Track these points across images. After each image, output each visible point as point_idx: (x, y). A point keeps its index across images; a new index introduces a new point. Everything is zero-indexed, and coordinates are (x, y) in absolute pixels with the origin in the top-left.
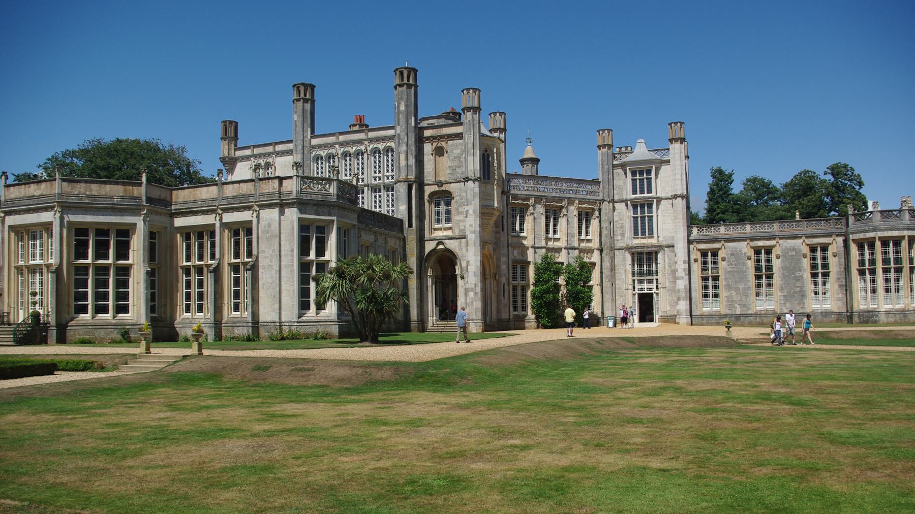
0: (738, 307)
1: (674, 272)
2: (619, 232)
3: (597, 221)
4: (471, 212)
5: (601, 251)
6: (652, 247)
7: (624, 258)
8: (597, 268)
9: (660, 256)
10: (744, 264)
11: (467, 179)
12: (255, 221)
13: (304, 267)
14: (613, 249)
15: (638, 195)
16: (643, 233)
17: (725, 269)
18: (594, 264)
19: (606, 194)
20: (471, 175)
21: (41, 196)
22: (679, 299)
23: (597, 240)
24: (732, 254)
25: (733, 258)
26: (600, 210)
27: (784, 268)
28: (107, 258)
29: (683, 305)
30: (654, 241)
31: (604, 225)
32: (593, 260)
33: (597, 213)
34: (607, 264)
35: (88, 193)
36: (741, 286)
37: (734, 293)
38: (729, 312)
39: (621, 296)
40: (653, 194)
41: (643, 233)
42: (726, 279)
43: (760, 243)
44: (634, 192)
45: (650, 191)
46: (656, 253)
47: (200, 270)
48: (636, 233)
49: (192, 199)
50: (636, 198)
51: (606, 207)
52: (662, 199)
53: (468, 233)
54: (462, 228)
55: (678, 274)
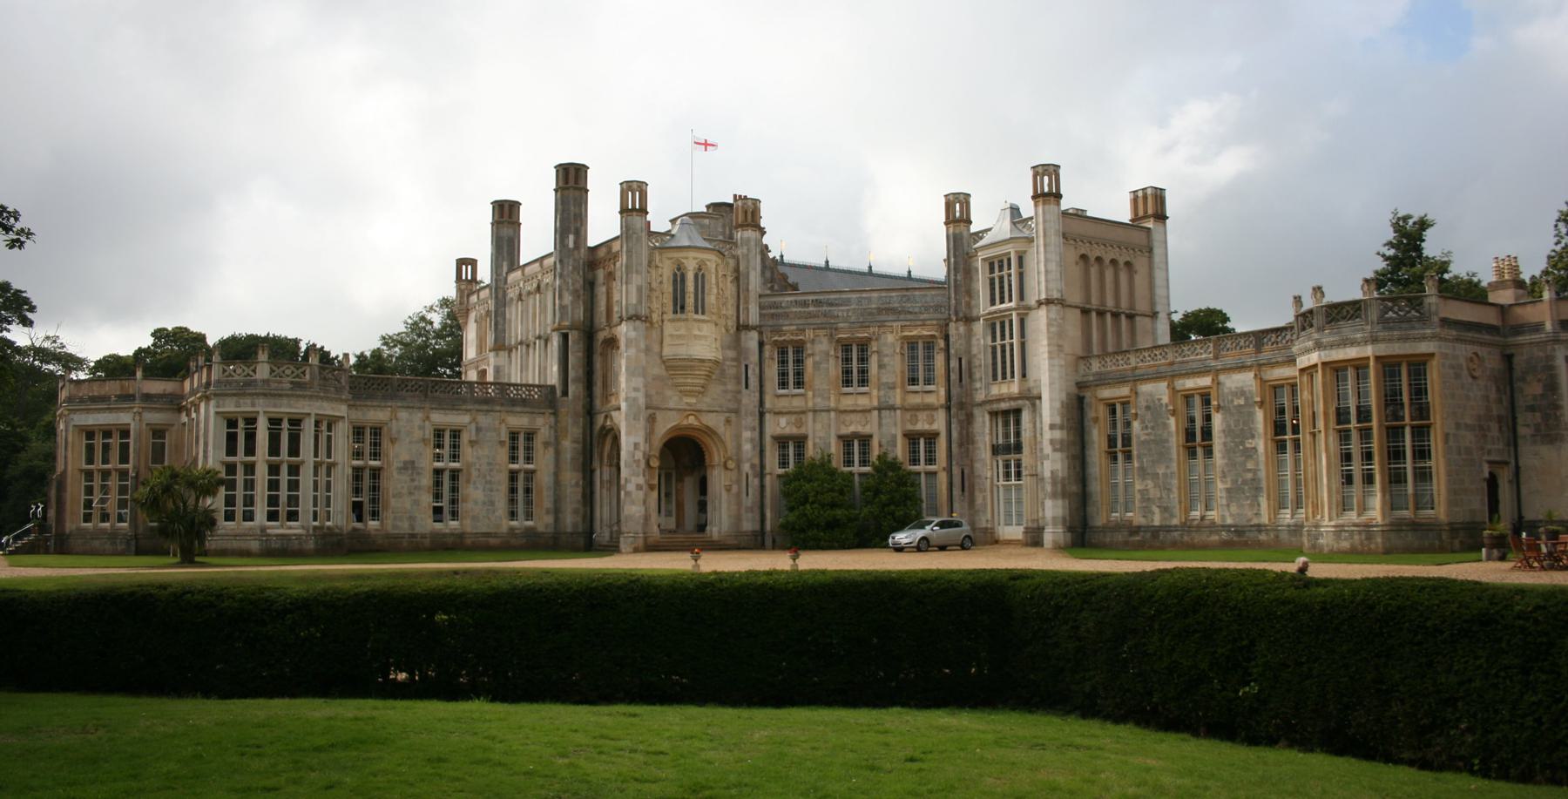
0: (1156, 510)
5: (948, 408)
6: (1011, 399)
8: (942, 444)
10: (1165, 426)
16: (1004, 377)
18: (936, 435)
23: (942, 392)
24: (1148, 408)
26: (947, 338)
27: (1228, 432)
29: (1053, 510)
31: (954, 363)
32: (935, 427)
33: (942, 343)
36: (1161, 471)
37: (1150, 484)
41: (1004, 377)
43: (1190, 383)
44: (993, 303)
46: (1018, 412)
47: (106, 475)
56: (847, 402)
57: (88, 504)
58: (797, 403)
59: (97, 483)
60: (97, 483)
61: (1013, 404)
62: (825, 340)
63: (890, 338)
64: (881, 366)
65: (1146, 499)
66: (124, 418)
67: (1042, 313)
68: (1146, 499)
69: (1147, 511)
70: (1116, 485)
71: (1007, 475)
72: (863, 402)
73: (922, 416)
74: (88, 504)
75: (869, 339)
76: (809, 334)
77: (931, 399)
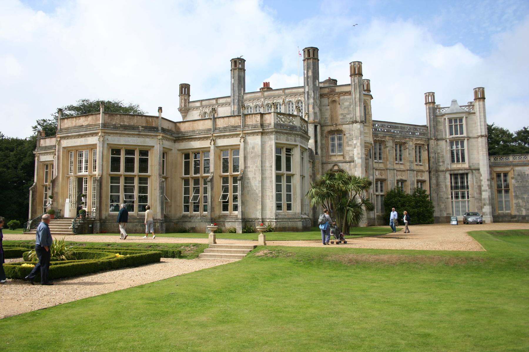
1: (480, 187)
2: (441, 160)
3: (426, 152)
4: (359, 144)
5: (430, 172)
7: (445, 178)
9: (470, 176)
11: (356, 122)
12: (242, 145)
13: (278, 178)
14: (437, 171)
15: (454, 136)
16: (458, 161)
17: (514, 185)
19: (432, 135)
20: (358, 119)
21: (89, 125)
22: (485, 205)
24: (519, 175)
25: (519, 178)
26: (428, 145)
28: (133, 171)
30: (466, 165)
32: (423, 178)
34: (434, 181)
35: (122, 124)
37: (520, 201)
38: (517, 213)
39: (443, 203)
40: (465, 134)
41: (458, 161)
42: (515, 192)
44: (451, 134)
45: (462, 133)
46: (467, 174)
48: (453, 161)
49: (191, 129)
50: (453, 138)
51: (432, 143)
52: (470, 138)
53: (356, 159)
54: (351, 155)
55: (483, 188)
56: (397, 167)
57: (186, 200)
58: (382, 166)
59: (192, 185)
60: (192, 185)
61: (466, 171)
62: (391, 141)
63: (411, 143)
64: (409, 154)
65: (518, 205)
66: (148, 142)
67: (480, 139)
68: (518, 205)
69: (519, 210)
70: (501, 202)
71: (457, 197)
72: (402, 167)
73: (419, 174)
74: (186, 200)
75: (405, 143)
76: (387, 138)
77: (422, 168)
